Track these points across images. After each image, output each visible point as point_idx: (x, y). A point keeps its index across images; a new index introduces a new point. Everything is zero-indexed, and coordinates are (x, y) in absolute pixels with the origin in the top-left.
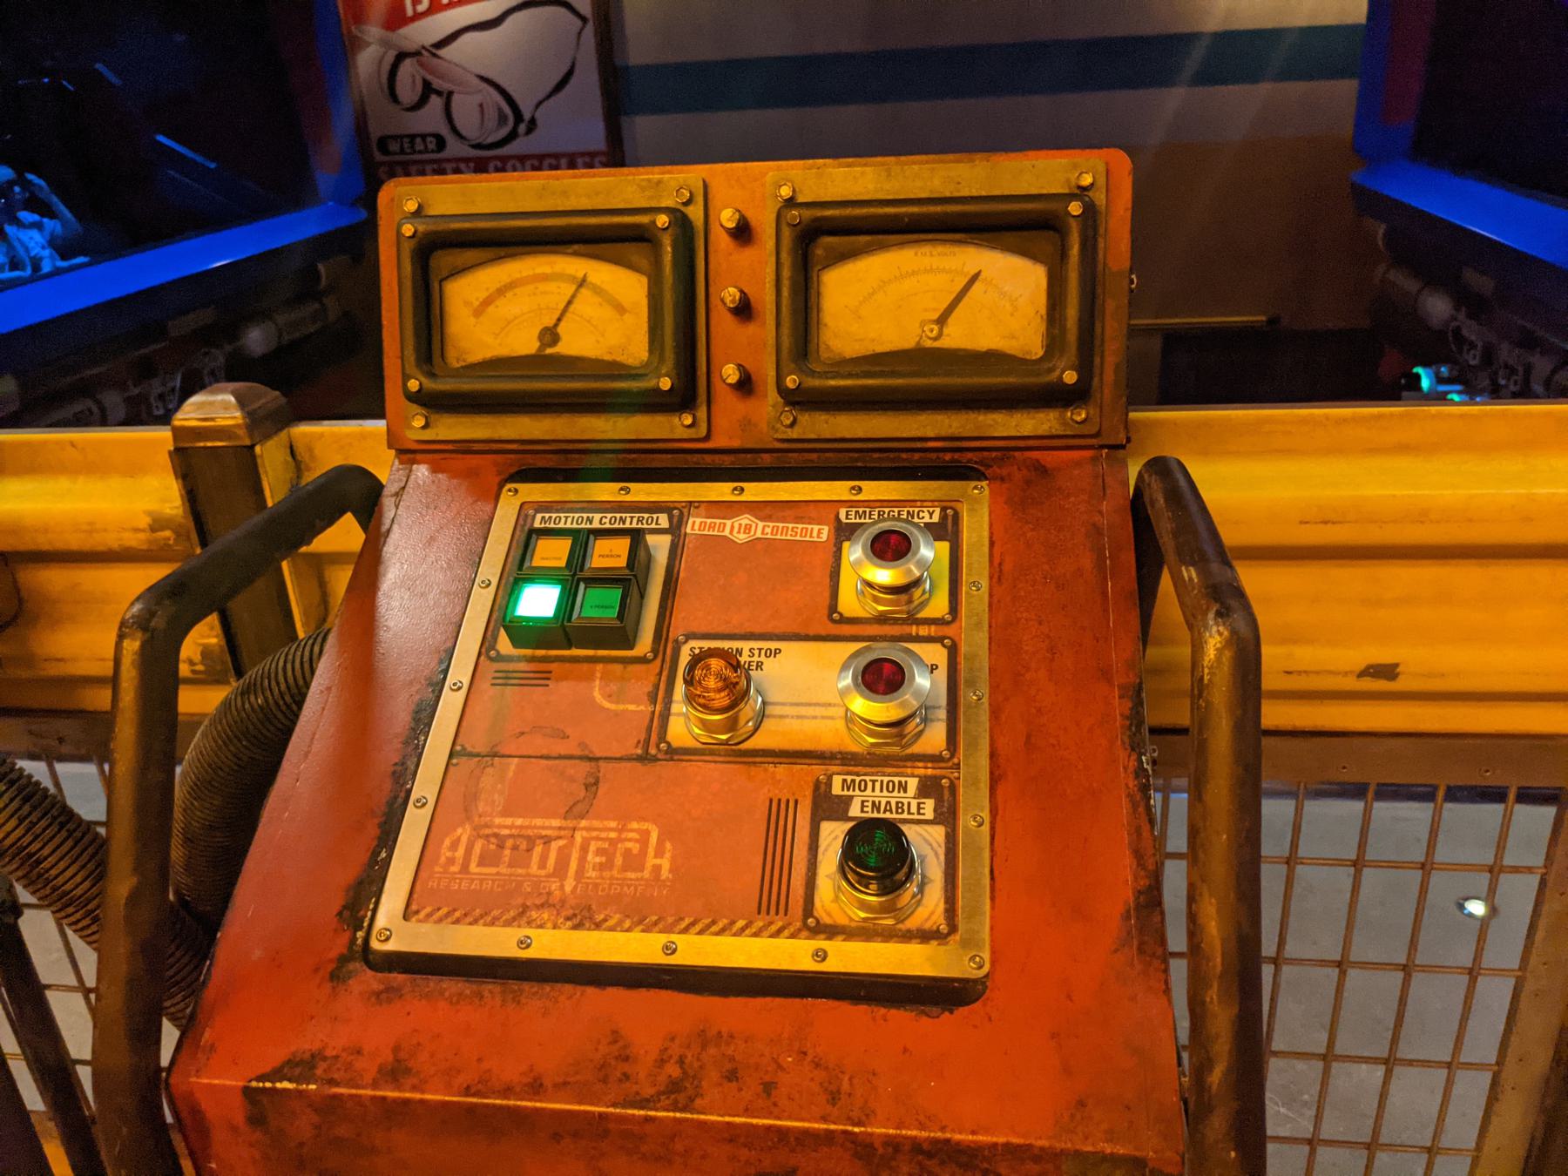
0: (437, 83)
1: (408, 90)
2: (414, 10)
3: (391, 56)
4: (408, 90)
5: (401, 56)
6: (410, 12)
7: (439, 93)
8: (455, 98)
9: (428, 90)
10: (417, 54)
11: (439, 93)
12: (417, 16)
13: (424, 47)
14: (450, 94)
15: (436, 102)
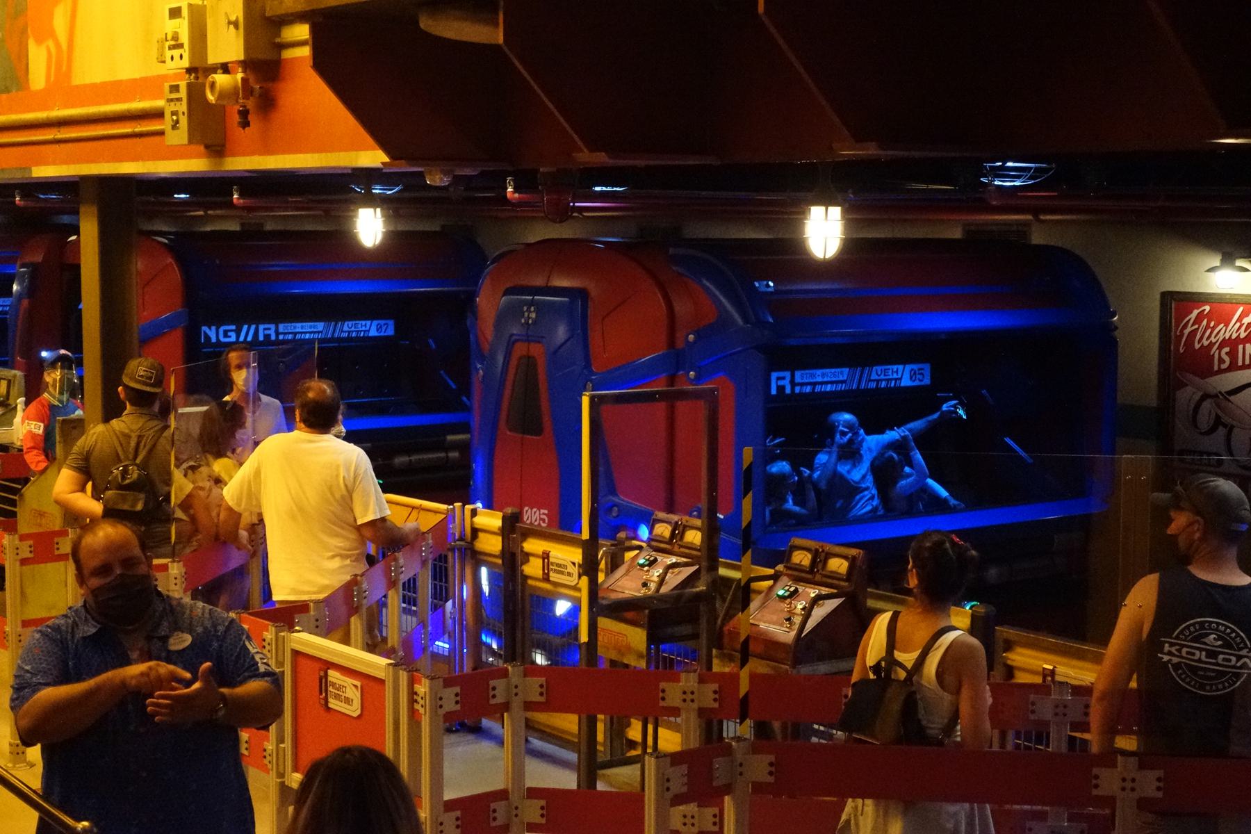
0: (1225, 419)
1: (1205, 419)
2: (1219, 365)
3: (1200, 394)
4: (1205, 419)
5: (1205, 396)
6: (1216, 368)
7: (1225, 426)
8: (1236, 431)
9: (1218, 422)
10: (1216, 396)
11: (1225, 426)
12: (1220, 371)
13: (1220, 392)
14: (1232, 427)
15: (1221, 431)
